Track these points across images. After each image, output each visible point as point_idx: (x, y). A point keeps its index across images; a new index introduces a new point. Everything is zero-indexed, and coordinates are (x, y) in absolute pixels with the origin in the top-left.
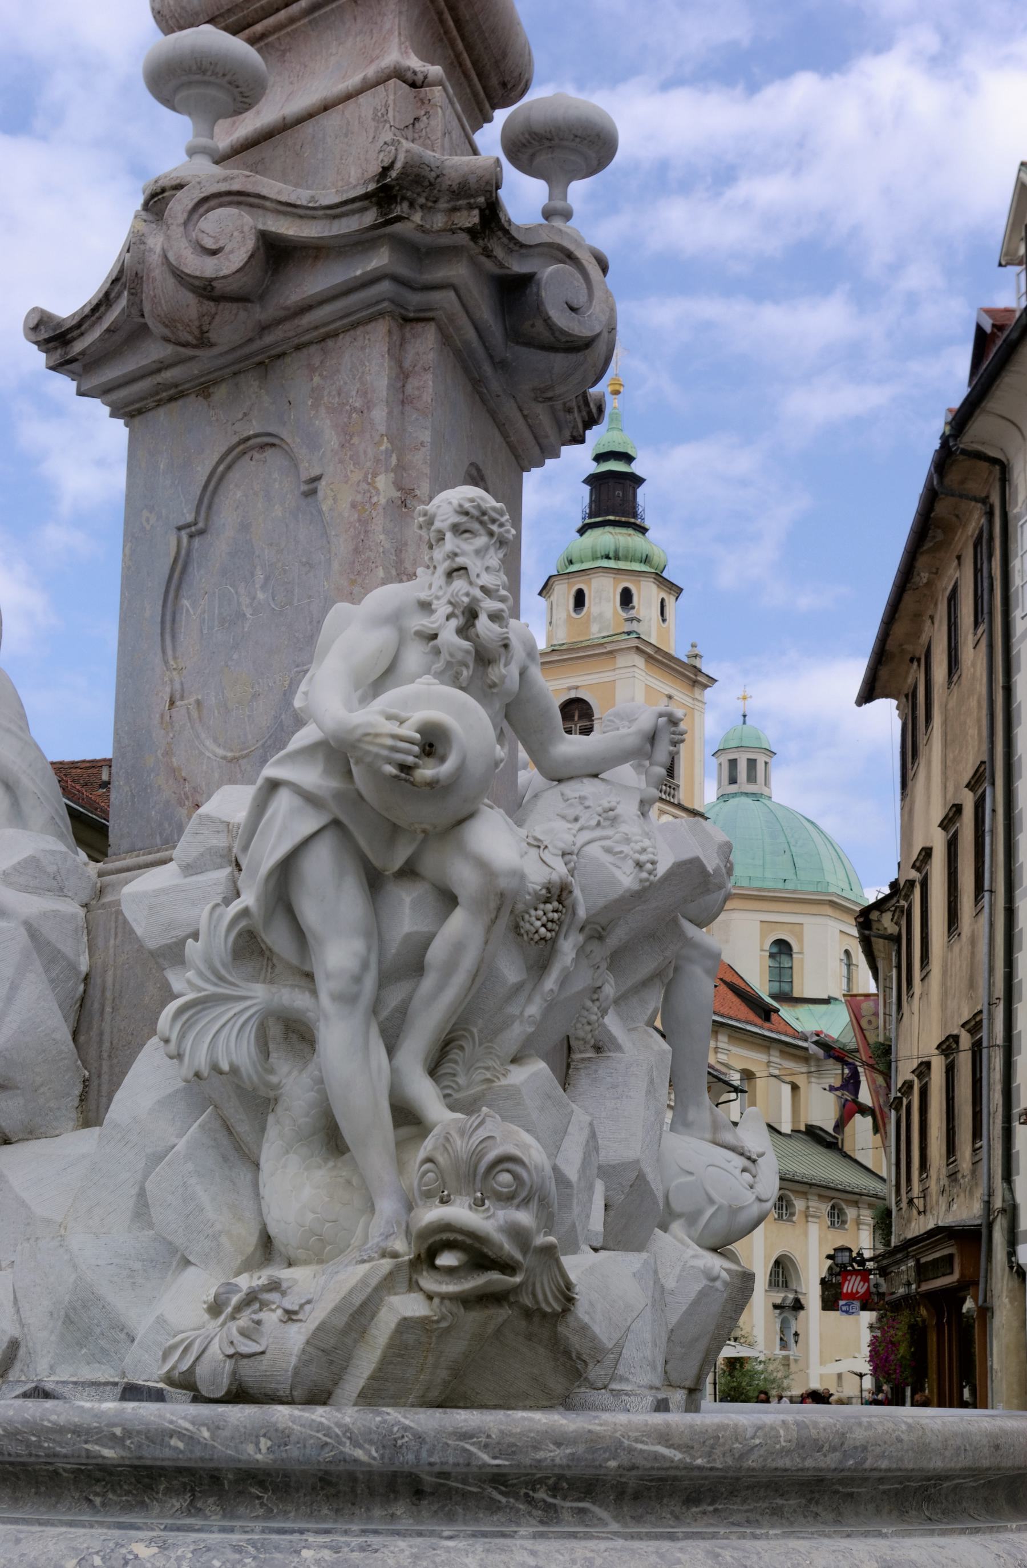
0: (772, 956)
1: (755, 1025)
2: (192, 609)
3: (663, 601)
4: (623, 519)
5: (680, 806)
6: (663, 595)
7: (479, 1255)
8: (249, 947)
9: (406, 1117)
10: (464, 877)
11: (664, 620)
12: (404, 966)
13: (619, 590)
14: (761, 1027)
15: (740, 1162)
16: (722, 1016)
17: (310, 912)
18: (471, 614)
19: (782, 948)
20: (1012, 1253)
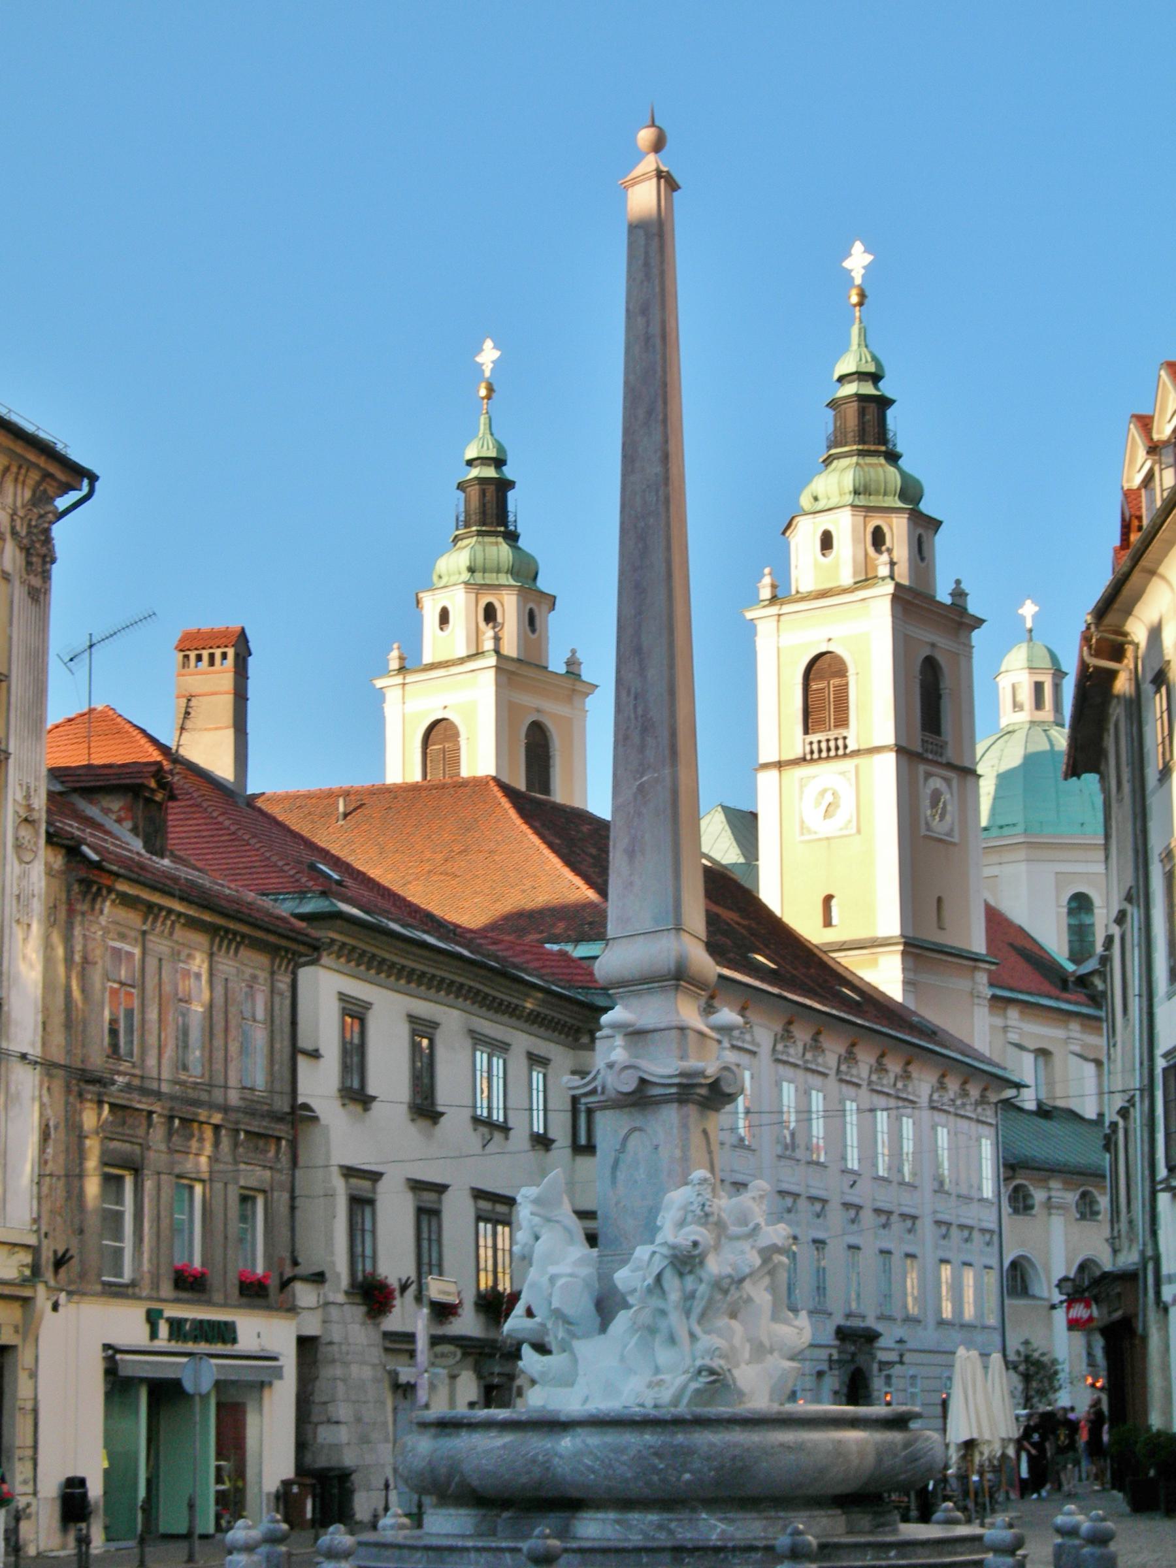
0: (1071, 912)
1: (1050, 997)
2: (621, 1176)
3: (920, 537)
4: (873, 448)
5: (950, 766)
6: (920, 531)
7: (712, 1372)
8: (650, 1291)
9: (693, 1336)
10: (704, 1275)
11: (922, 559)
12: (690, 1296)
13: (870, 529)
14: (1057, 999)
15: (796, 1331)
16: (1011, 989)
17: (666, 1285)
18: (703, 1205)
19: (1080, 904)
20: (1158, 1293)
